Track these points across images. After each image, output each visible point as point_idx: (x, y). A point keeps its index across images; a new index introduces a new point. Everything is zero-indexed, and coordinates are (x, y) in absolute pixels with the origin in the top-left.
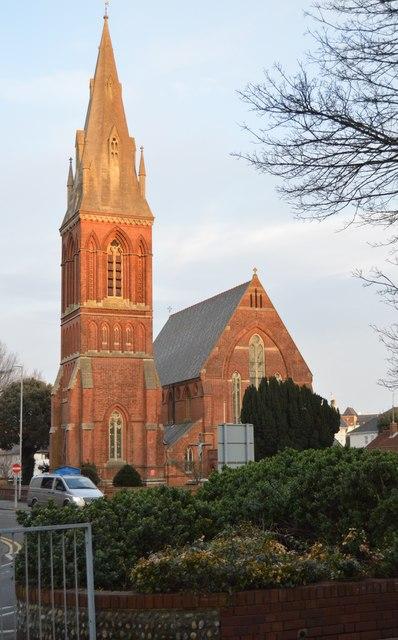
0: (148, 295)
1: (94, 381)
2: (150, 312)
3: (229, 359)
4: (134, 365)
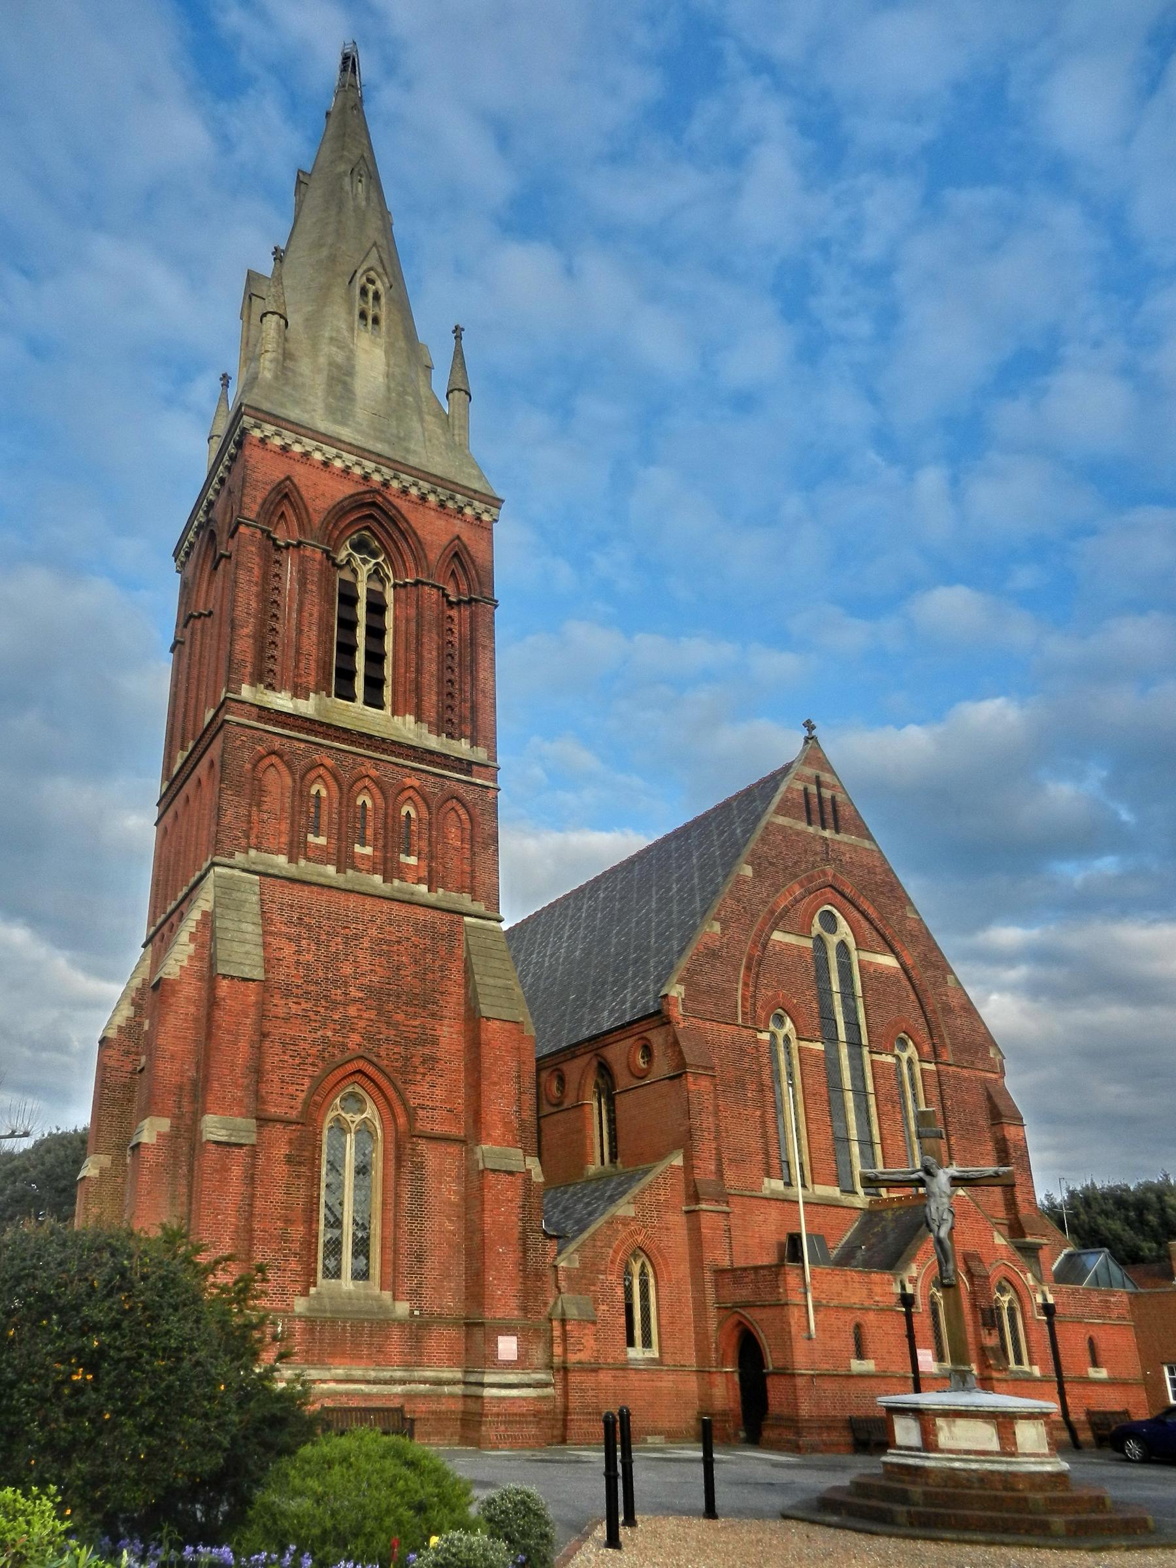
0: (482, 718)
1: (269, 963)
2: (490, 768)
3: (755, 966)
4: (423, 929)
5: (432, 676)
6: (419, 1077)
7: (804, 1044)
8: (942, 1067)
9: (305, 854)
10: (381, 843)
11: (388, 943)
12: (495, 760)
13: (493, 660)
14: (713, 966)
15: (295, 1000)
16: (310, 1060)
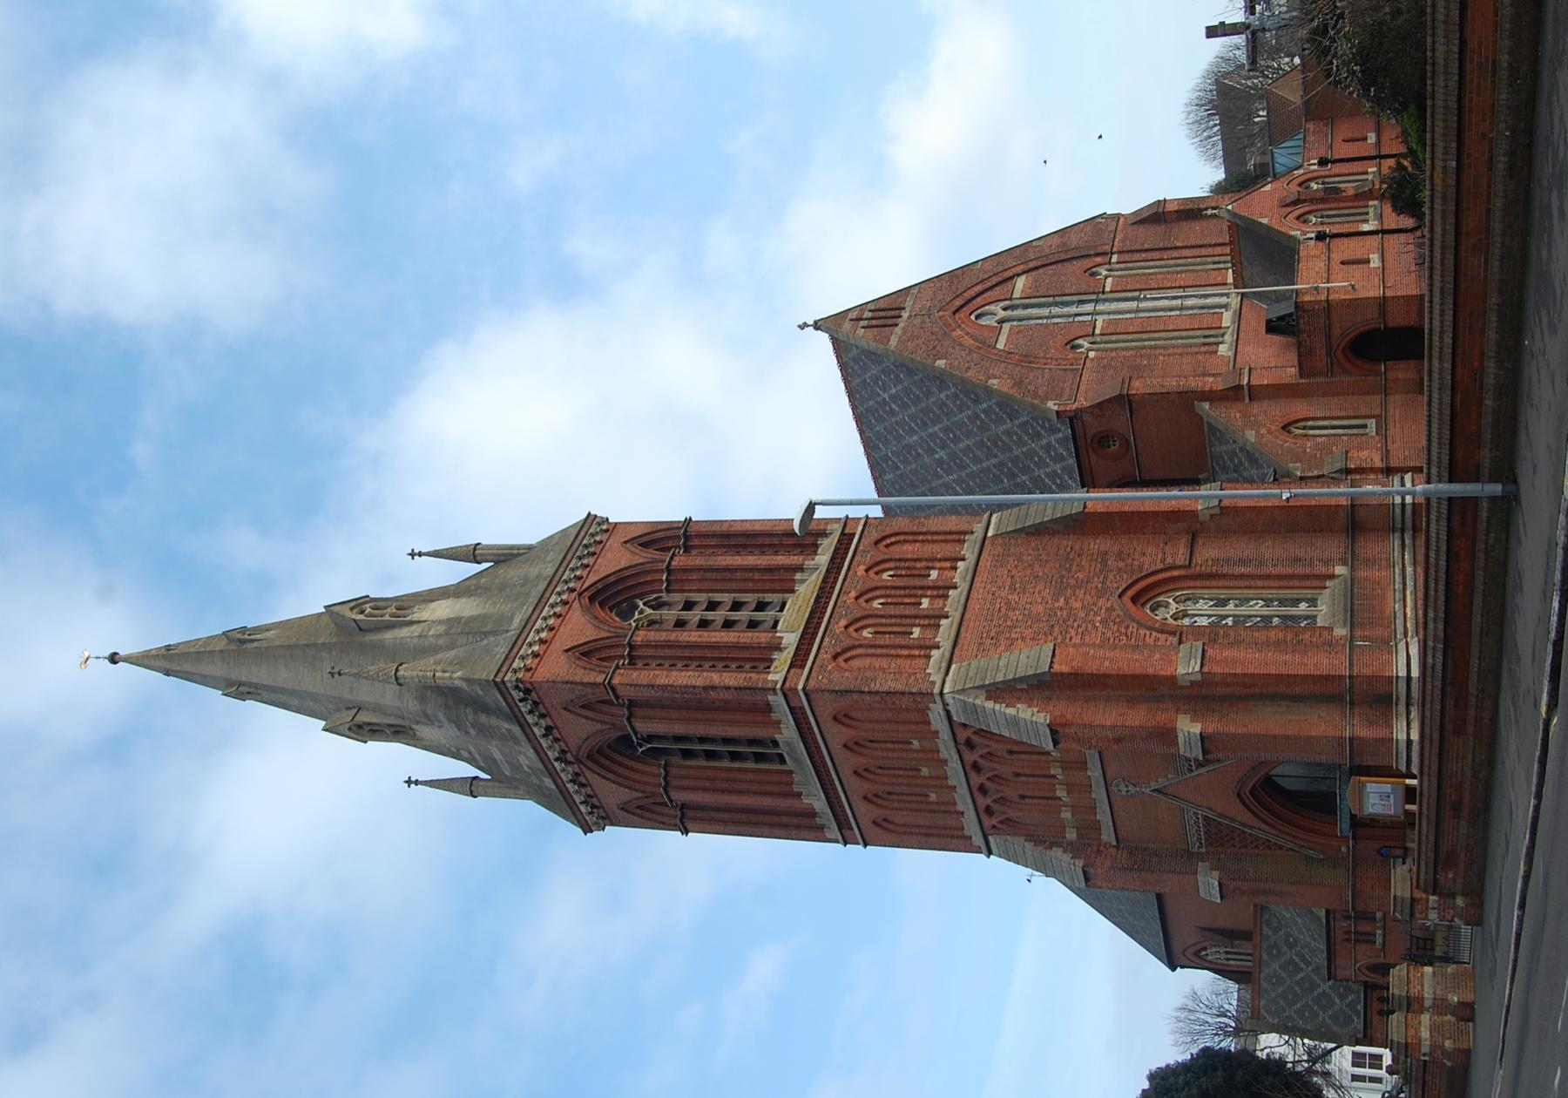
5: (759, 559)
6: (1136, 563)
7: (1097, 331)
8: (1115, 250)
9: (930, 639)
10: (920, 592)
11: (1013, 584)
12: (840, 519)
13: (743, 521)
14: (1029, 384)
15: (1068, 640)
16: (1123, 630)
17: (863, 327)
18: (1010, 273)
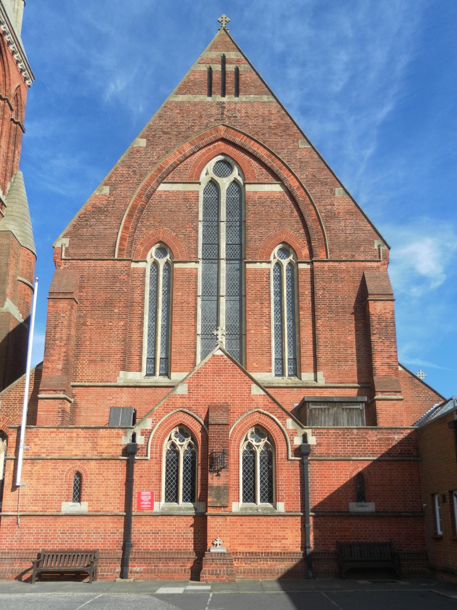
17: (210, 69)
18: (284, 174)
